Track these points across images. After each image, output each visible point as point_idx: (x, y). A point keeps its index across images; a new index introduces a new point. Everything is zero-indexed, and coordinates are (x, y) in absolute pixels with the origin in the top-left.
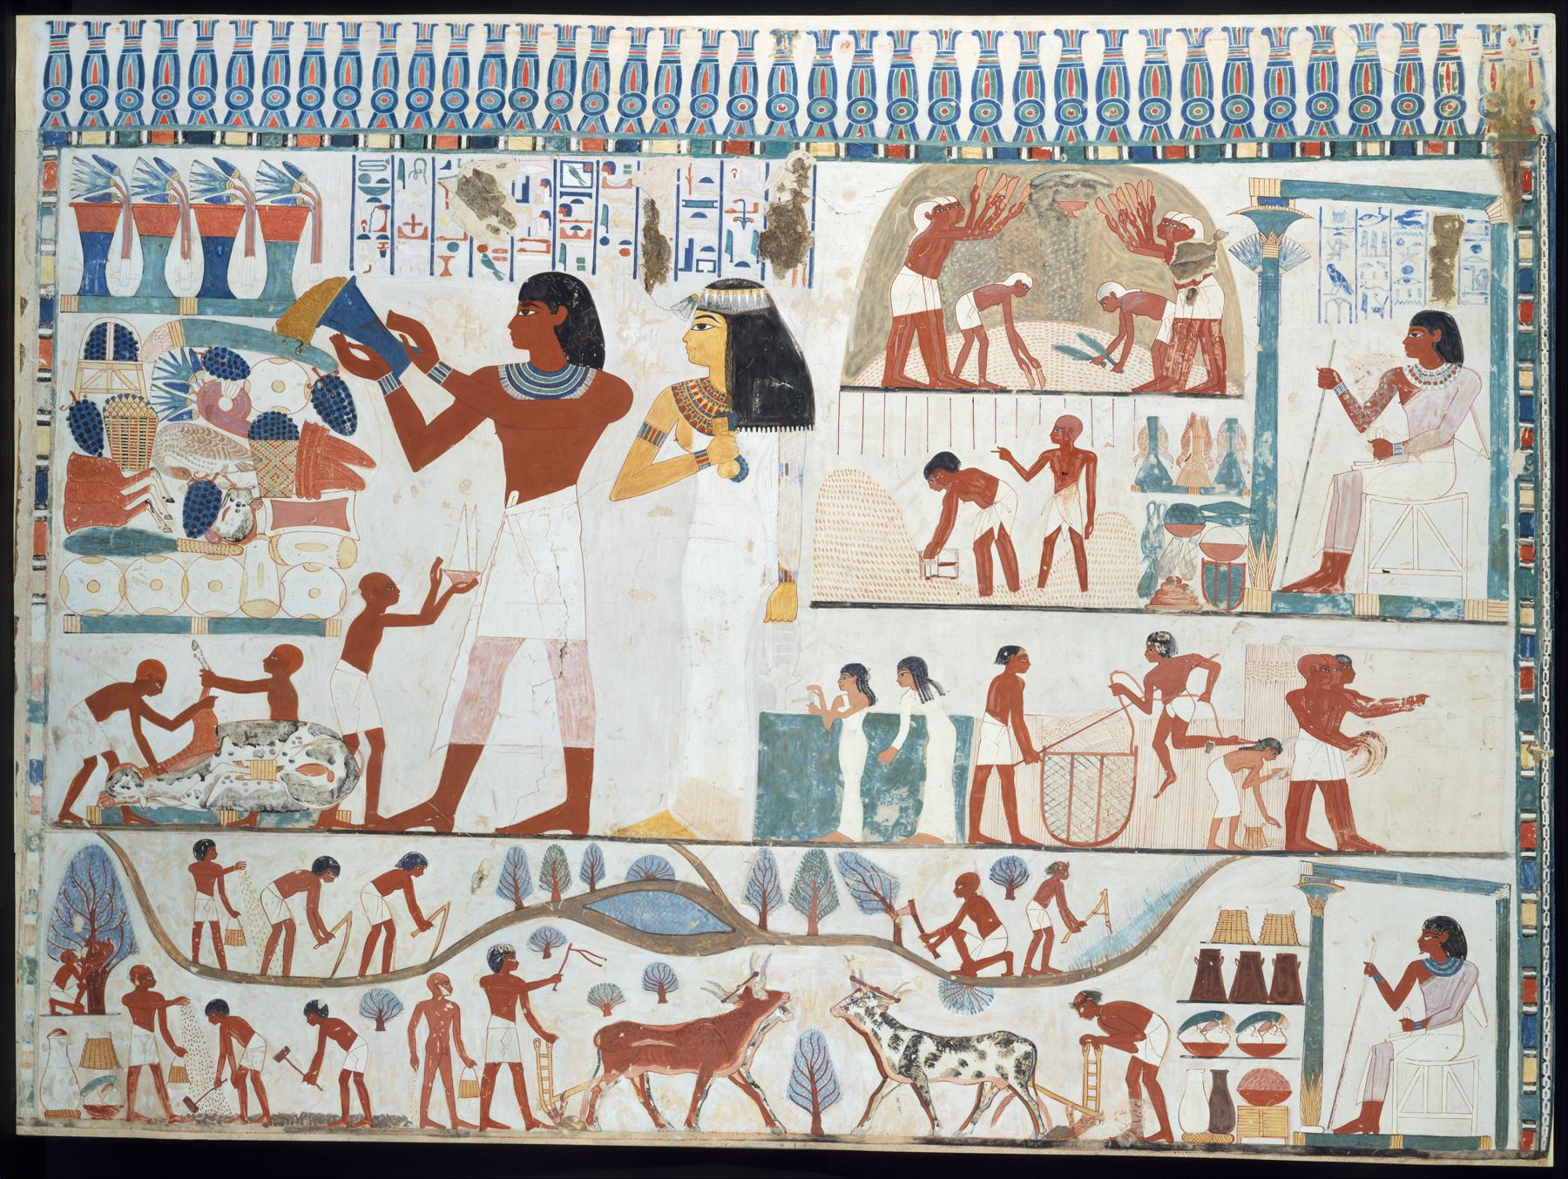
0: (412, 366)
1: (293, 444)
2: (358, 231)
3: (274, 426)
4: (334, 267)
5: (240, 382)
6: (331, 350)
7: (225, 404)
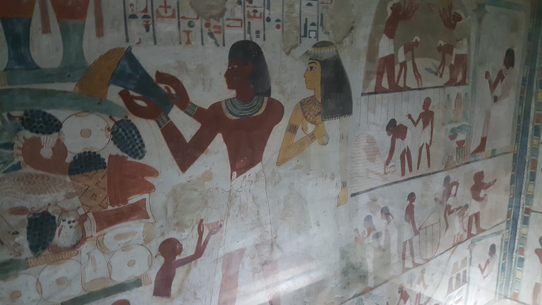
0: (175, 106)
1: (101, 173)
2: (129, 12)
3: (88, 162)
4: (113, 39)
5: (55, 135)
6: (120, 102)
7: (47, 152)
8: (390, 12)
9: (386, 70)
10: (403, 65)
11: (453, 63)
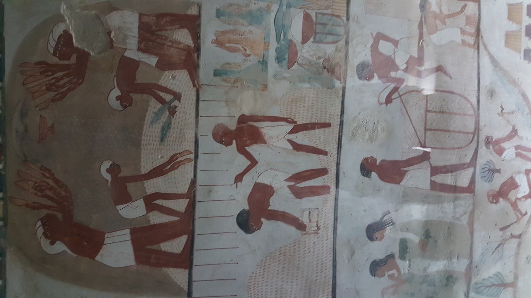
8: (60, 247)
9: (155, 247)
10: (151, 202)
11: (153, 60)
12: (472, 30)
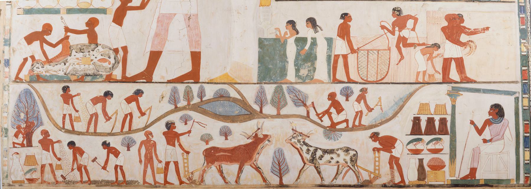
12: (427, 79)
